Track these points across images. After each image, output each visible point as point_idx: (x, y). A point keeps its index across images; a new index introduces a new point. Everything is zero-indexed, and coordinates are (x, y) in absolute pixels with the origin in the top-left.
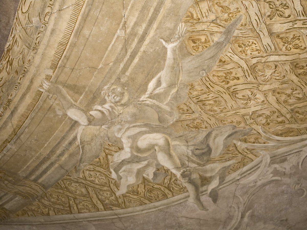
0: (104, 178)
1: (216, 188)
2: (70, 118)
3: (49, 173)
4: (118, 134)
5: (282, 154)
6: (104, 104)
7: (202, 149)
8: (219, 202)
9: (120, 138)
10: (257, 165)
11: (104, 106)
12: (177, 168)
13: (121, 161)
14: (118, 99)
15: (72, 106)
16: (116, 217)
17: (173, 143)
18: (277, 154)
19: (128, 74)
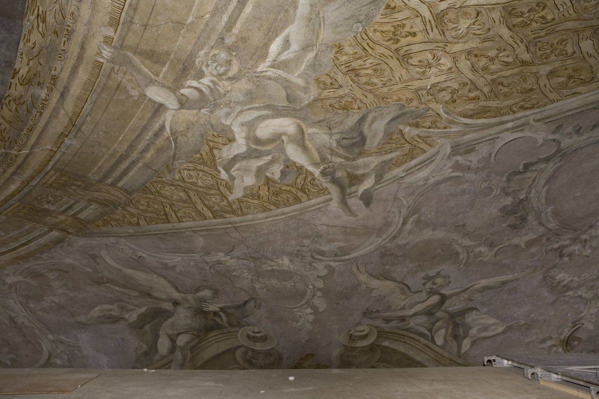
0: (210, 179)
1: (370, 188)
2: (150, 100)
3: (130, 174)
4: (226, 120)
5: (469, 142)
6: (201, 78)
7: (352, 138)
8: (373, 206)
9: (230, 126)
10: (431, 157)
11: (201, 81)
12: (316, 164)
13: (232, 156)
14: (222, 70)
15: (151, 82)
16: (230, 226)
17: (309, 131)
18: (462, 142)
19: (235, 31)
